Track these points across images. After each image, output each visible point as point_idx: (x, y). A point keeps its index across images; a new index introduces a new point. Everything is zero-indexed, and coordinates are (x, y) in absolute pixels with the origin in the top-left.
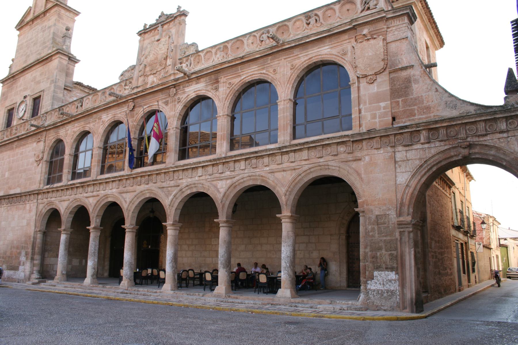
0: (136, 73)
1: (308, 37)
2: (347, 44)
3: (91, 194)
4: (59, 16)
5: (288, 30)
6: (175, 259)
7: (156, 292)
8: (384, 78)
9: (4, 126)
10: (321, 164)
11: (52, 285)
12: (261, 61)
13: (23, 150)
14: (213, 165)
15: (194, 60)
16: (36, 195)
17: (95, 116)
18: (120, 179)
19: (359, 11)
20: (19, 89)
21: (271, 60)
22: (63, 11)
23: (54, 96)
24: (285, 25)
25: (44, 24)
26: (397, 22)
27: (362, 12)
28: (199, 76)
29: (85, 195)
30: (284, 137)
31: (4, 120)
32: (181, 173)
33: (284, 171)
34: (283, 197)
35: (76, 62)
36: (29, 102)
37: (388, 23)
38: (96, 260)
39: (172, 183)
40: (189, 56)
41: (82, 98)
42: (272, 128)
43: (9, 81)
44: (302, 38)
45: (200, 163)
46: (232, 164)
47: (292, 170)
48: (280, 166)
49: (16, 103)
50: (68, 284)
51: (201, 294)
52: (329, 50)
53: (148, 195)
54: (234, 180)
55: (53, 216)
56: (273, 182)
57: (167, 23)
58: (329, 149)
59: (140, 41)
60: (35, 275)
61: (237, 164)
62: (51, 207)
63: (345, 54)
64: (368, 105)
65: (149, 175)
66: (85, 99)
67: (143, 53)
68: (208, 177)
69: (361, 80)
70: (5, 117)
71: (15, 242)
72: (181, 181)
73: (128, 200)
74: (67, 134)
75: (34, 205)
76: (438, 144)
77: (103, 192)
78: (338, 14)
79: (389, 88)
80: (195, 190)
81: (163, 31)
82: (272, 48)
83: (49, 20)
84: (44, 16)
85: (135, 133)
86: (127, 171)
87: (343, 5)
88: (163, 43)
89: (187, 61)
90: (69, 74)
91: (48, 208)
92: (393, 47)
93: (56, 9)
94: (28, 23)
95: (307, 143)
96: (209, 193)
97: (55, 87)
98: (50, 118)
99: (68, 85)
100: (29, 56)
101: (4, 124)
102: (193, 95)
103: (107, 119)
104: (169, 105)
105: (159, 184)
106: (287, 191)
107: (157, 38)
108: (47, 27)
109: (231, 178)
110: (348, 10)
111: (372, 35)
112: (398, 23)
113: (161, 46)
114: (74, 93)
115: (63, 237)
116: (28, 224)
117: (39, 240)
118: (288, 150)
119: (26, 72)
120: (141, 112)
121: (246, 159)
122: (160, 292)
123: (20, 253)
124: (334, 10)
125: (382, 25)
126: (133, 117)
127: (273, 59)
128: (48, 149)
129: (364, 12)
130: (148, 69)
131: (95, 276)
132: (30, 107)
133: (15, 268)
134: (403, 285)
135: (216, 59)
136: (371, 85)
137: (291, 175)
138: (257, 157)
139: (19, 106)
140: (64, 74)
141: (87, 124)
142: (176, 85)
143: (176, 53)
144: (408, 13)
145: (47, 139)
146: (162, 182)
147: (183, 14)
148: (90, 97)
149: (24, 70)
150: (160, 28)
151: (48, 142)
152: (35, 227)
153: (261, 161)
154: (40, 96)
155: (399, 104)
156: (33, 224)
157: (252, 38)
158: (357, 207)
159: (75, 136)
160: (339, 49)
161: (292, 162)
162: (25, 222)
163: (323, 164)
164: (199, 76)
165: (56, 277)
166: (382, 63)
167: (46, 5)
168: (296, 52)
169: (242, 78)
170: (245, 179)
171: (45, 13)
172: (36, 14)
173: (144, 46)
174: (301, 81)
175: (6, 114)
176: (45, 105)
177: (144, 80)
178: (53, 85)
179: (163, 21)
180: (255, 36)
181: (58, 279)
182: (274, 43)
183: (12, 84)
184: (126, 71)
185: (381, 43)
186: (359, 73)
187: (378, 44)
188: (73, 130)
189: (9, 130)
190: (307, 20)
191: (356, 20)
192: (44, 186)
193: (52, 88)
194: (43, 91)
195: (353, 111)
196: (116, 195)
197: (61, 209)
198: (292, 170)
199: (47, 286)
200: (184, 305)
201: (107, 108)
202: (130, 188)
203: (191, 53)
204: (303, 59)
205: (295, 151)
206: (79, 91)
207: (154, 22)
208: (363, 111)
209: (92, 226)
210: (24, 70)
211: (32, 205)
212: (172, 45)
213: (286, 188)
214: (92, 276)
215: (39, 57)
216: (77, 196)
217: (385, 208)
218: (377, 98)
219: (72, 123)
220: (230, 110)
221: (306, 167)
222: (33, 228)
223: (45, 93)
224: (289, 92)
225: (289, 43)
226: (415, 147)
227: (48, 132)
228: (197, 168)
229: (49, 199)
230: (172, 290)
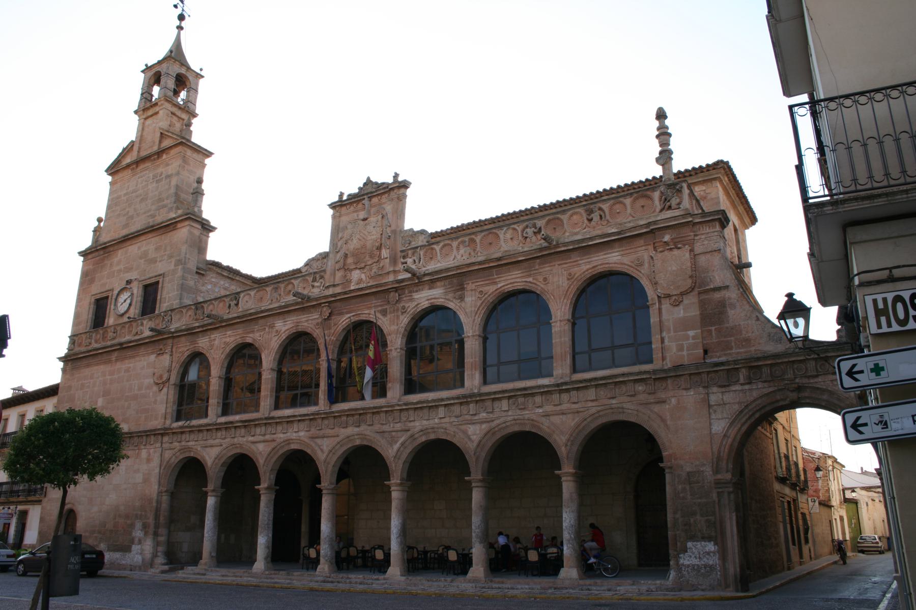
0: (329, 264)
1: (591, 239)
2: (643, 252)
3: (261, 438)
4: (185, 160)
5: (563, 225)
6: (404, 532)
7: (378, 579)
8: (691, 300)
9: (89, 324)
10: (613, 406)
11: (198, 574)
12: (525, 264)
13: (131, 365)
14: (461, 404)
15: (425, 255)
16: (160, 437)
17: (261, 322)
18: (312, 419)
19: (658, 210)
20: (116, 268)
21: (540, 264)
22: (189, 152)
23: (182, 284)
24: (558, 218)
25: (160, 170)
26: (706, 229)
27: (661, 211)
28: (433, 279)
29: (251, 439)
30: (561, 370)
31: (90, 316)
32: (411, 412)
33: (563, 414)
34: (563, 448)
35: (211, 231)
36: (137, 290)
37: (695, 229)
38: (271, 535)
39: (398, 426)
40: (417, 247)
41: (238, 293)
42: (543, 355)
43: (97, 254)
44: (583, 240)
45: (442, 400)
46: (489, 403)
47: (574, 413)
48: (558, 408)
49: (112, 290)
50: (224, 571)
51: (449, 579)
52: (619, 257)
53: (358, 442)
54: (494, 424)
55: (191, 469)
56: (548, 427)
57: (378, 195)
58: (624, 388)
59: (334, 217)
60: (160, 560)
61: (496, 404)
62: (187, 455)
63: (641, 265)
64: (672, 333)
65: (360, 414)
66: (242, 295)
67: (340, 235)
68: (453, 419)
69: (663, 301)
70: (91, 311)
71: (122, 508)
72: (412, 424)
73: (326, 449)
74: (212, 346)
75: (155, 452)
76: (760, 385)
77: (282, 435)
78: (629, 210)
79: (698, 313)
80: (432, 437)
81: (371, 206)
82: (541, 250)
83: (167, 165)
84: (158, 158)
85: (333, 352)
86: (323, 404)
87: (636, 199)
88: (374, 224)
89: (413, 254)
90: (202, 248)
91: (181, 457)
92: (702, 260)
93: (179, 149)
94: (128, 166)
95: (595, 379)
96: (455, 441)
97: (185, 270)
98: (179, 319)
99: (201, 266)
100: (132, 217)
101: (90, 321)
102: (425, 304)
103: (284, 329)
104: (389, 316)
105: (377, 427)
106: (568, 440)
107: (362, 215)
108: (163, 176)
109: (488, 422)
110: (643, 206)
111: (675, 244)
112: (708, 231)
113: (370, 228)
114: (208, 278)
115: (211, 501)
116: (146, 480)
117: (165, 505)
118: (568, 387)
119: (129, 243)
120: (344, 321)
121: (509, 398)
122: (384, 579)
123: (132, 526)
124: (625, 205)
125: (687, 232)
126: (330, 329)
127: (543, 264)
128: (178, 366)
129: (664, 212)
130: (350, 260)
131: (269, 559)
132: (139, 299)
133: (126, 549)
134: (723, 557)
135: (459, 257)
136: (676, 308)
137: (574, 419)
138: (525, 396)
139: (118, 295)
140: (196, 251)
141: (249, 333)
142: (400, 288)
143: (395, 240)
144: (720, 219)
145: (174, 350)
146: (382, 424)
147: (405, 185)
148: (252, 293)
149: (126, 240)
150: (366, 202)
151: (176, 356)
152: (159, 485)
153: (530, 399)
154: (158, 283)
155: (711, 334)
156: (154, 480)
157: (510, 231)
158: (662, 462)
159: (228, 350)
160: (634, 256)
161: (574, 403)
162: (139, 478)
163: (616, 406)
164: (433, 279)
165: (202, 561)
166: (690, 281)
167: (160, 142)
168: (575, 257)
169: (499, 285)
170: (508, 424)
171: (159, 153)
172: (144, 153)
173: (341, 225)
174: (582, 292)
175: (92, 306)
176: (168, 297)
177: (346, 276)
178: (180, 267)
179: (372, 193)
180: (514, 229)
181: (205, 564)
182: (546, 244)
183: (103, 260)
184: (313, 259)
185: (687, 255)
187: (684, 255)
188: (224, 340)
189: (101, 332)
190: (589, 215)
191: (655, 222)
192: (172, 422)
193: (180, 273)
194: (163, 275)
195: (653, 340)
196: (306, 440)
197: (207, 458)
198: (574, 413)
199: (188, 573)
200: (436, 594)
201: (284, 312)
202: (331, 432)
203: (420, 244)
204: (584, 268)
205: (578, 389)
206: (214, 275)
207: (355, 191)
208: (666, 341)
209: (263, 485)
210: (126, 240)
211: (151, 451)
212: (388, 229)
213: (567, 436)
214: (266, 559)
215: (151, 222)
216: (236, 440)
217: (698, 463)
218: (684, 324)
219: (221, 329)
220: (481, 329)
221: (594, 410)
222: (156, 487)
223: (167, 279)
224: (567, 311)
225: (565, 244)
226: (733, 388)
227: (176, 340)
228: (437, 407)
229: (183, 443)
230: (402, 575)
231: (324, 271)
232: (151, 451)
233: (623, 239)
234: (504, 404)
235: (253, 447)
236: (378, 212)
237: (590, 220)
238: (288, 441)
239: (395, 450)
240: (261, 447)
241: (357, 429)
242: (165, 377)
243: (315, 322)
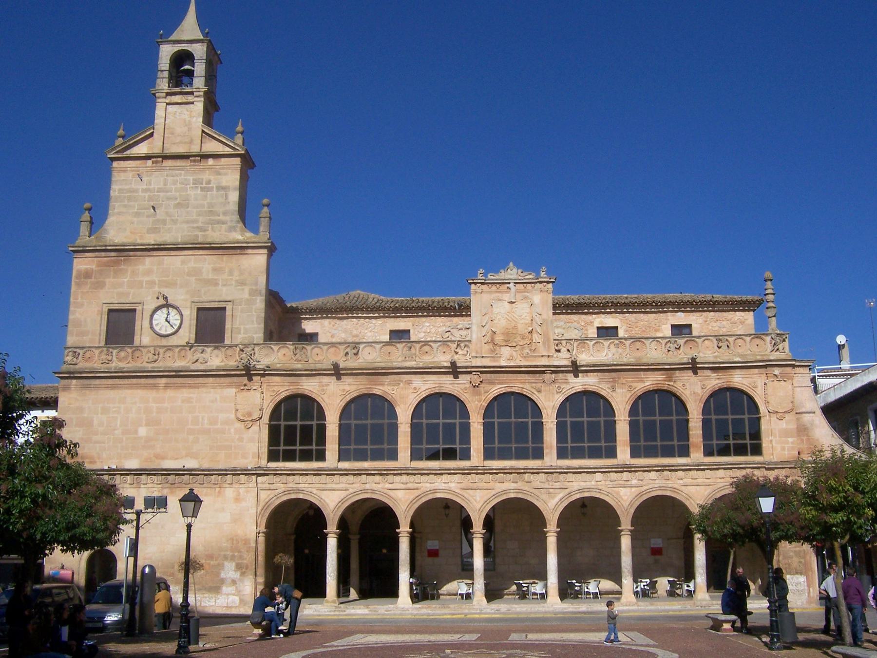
3: (403, 486)
19: (769, 350)
29: (388, 486)
39: (557, 485)
75: (247, 492)
134: (809, 586)
157: (655, 342)
160: (750, 380)
185: (790, 387)
186: (771, 408)
218: (786, 433)
229: (291, 485)
231: (470, 341)
232: (241, 491)
233: (745, 367)
234: (653, 475)
235: (391, 493)
236: (526, 298)
237: (719, 348)
238: (435, 491)
239: (552, 506)
240: (400, 494)
241: (513, 485)
242: (256, 416)
243: (463, 386)
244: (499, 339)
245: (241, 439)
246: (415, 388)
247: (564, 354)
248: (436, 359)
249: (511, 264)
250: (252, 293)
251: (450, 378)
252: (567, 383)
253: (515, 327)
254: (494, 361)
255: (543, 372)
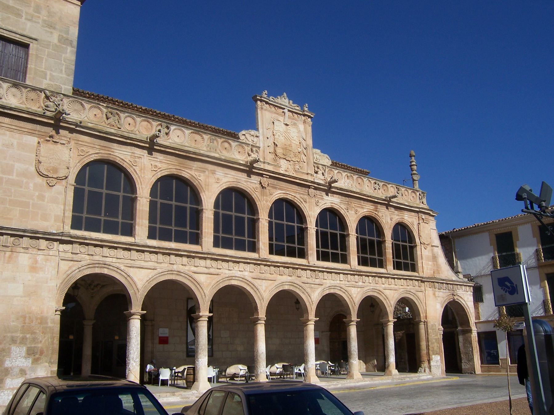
3: (206, 271)
39: (317, 281)
75: (47, 260)
229: (97, 258)
232: (40, 258)
239: (312, 298)
241: (290, 278)
244: (279, 151)
245: (41, 197)
246: (218, 179)
247: (320, 175)
248: (233, 156)
249: (285, 94)
250: (64, 40)
251: (244, 175)
252: (322, 199)
253: (290, 145)
254: (276, 169)
255: (309, 187)
